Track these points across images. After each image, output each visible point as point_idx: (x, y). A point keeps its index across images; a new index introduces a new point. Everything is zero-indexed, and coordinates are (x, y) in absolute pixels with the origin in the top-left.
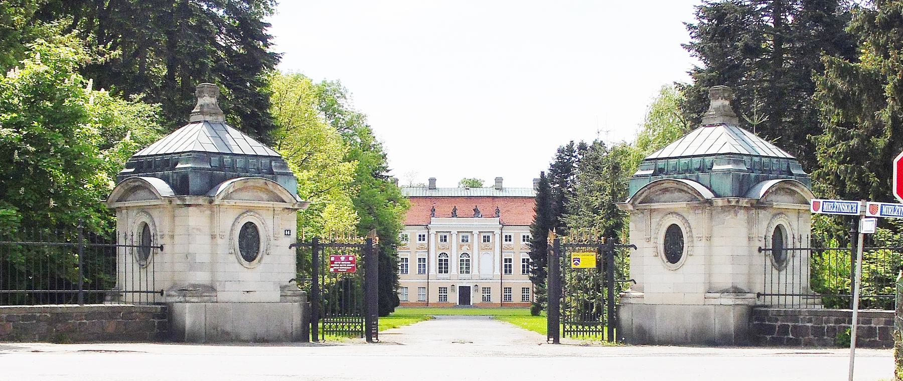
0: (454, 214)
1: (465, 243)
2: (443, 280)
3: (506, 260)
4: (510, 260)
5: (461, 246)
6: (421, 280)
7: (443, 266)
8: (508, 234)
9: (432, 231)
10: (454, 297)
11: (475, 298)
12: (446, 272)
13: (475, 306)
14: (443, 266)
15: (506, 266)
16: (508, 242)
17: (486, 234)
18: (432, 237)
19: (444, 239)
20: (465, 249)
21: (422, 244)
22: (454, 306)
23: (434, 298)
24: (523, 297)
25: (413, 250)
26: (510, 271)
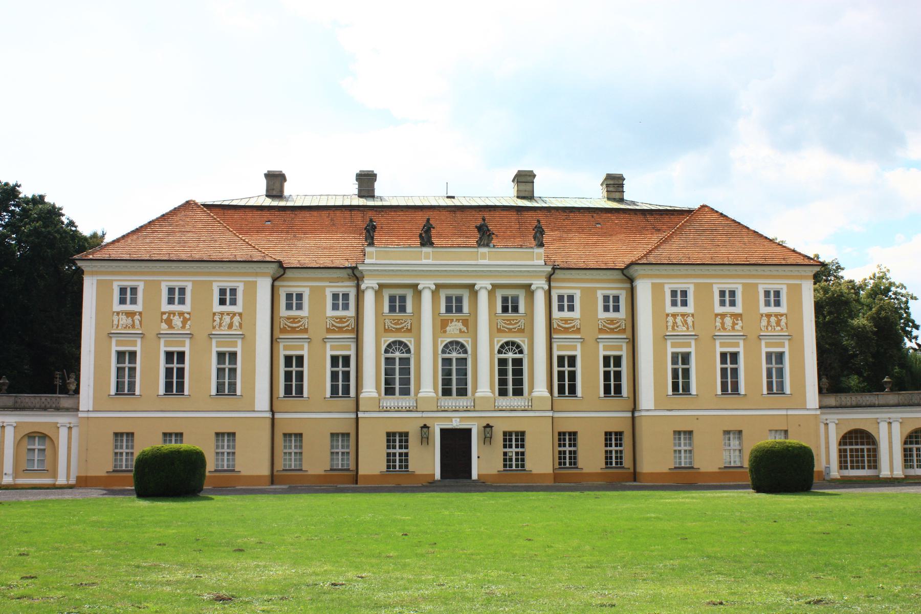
0: (426, 240)
1: (454, 315)
2: (397, 413)
3: (561, 359)
4: (572, 360)
5: (444, 324)
6: (338, 416)
7: (397, 378)
8: (566, 292)
9: (369, 283)
10: (428, 461)
11: (484, 461)
12: (405, 392)
13: (485, 485)
14: (397, 378)
15: (561, 375)
16: (566, 314)
17: (510, 293)
18: (369, 299)
19: (397, 304)
20: (454, 330)
21: (341, 319)
22: (430, 486)
23: (373, 461)
24: (608, 458)
25: (317, 332)
26: (573, 390)
